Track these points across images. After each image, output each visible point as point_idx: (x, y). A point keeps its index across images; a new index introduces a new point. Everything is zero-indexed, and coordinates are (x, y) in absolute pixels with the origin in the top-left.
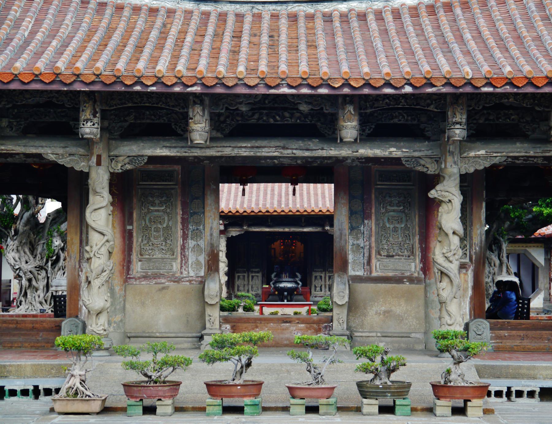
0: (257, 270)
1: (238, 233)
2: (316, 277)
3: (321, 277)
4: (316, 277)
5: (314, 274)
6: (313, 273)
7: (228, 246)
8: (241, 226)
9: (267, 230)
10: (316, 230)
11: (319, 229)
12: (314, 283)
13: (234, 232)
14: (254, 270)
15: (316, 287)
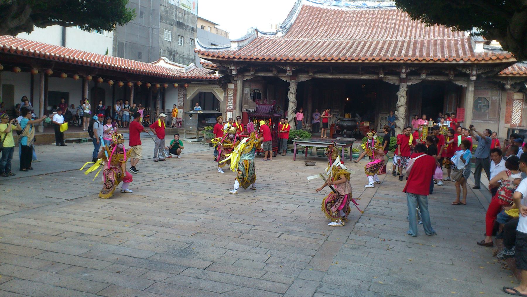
0: (337, 110)
1: (306, 79)
2: (382, 118)
3: (386, 118)
4: (382, 118)
5: (381, 115)
6: (380, 114)
7: (298, 90)
8: (307, 72)
9: (330, 77)
10: (373, 78)
11: (375, 77)
12: (380, 122)
13: (303, 78)
14: (335, 110)
15: (381, 125)
